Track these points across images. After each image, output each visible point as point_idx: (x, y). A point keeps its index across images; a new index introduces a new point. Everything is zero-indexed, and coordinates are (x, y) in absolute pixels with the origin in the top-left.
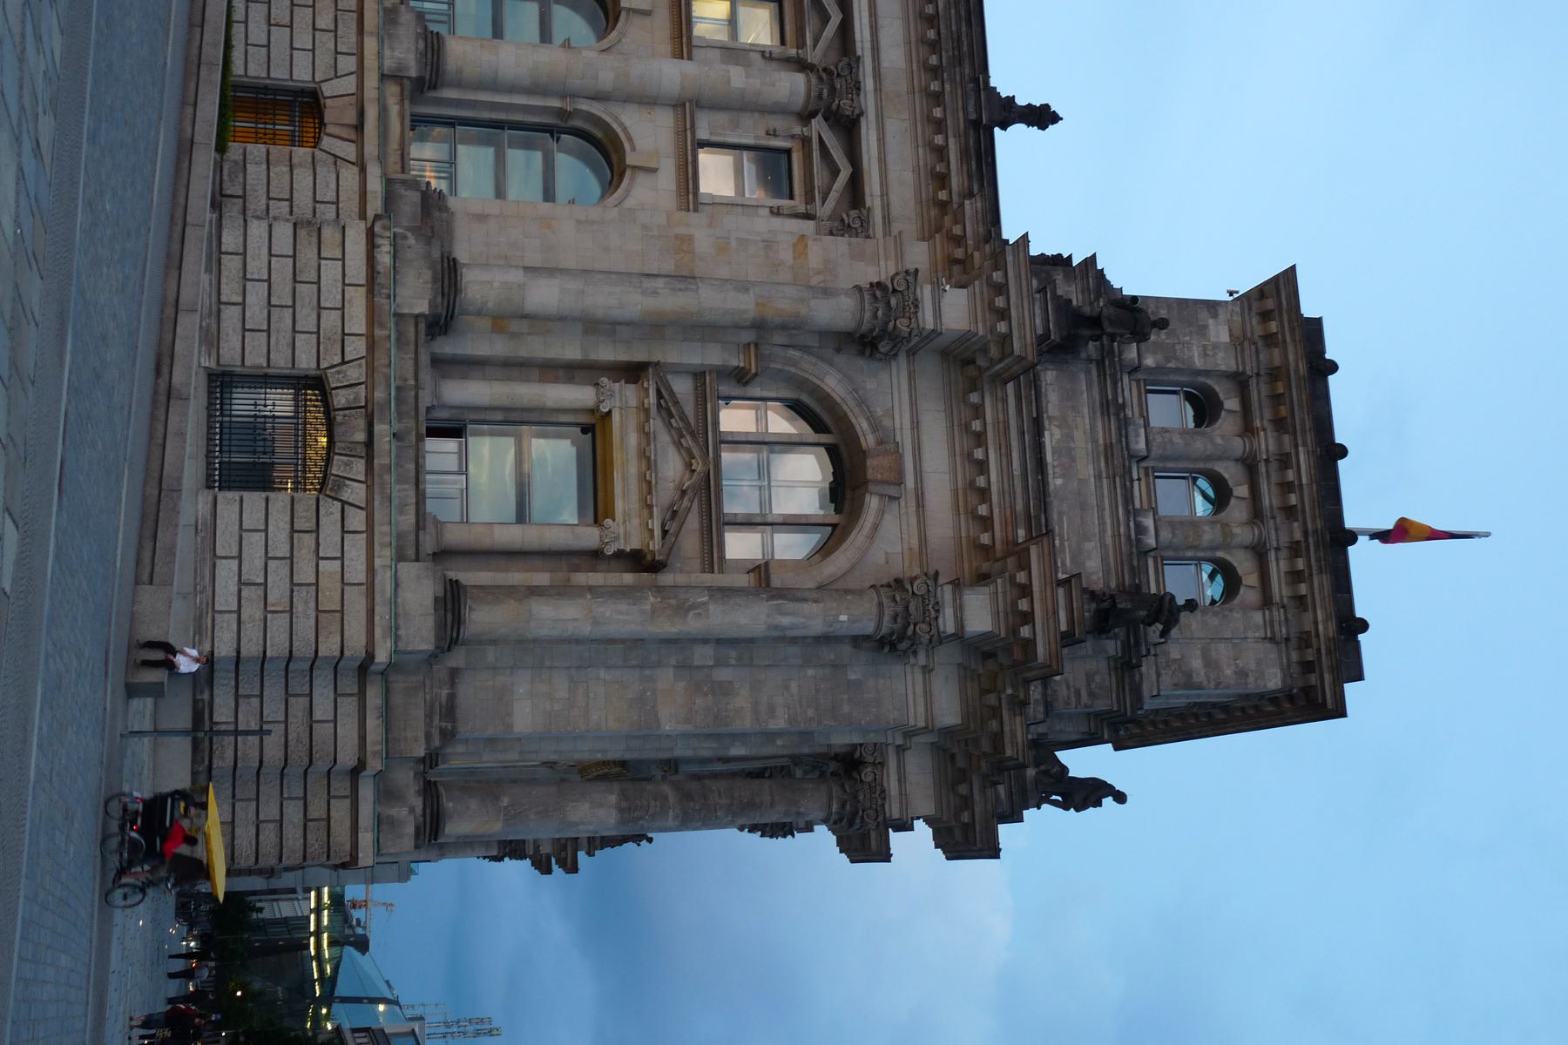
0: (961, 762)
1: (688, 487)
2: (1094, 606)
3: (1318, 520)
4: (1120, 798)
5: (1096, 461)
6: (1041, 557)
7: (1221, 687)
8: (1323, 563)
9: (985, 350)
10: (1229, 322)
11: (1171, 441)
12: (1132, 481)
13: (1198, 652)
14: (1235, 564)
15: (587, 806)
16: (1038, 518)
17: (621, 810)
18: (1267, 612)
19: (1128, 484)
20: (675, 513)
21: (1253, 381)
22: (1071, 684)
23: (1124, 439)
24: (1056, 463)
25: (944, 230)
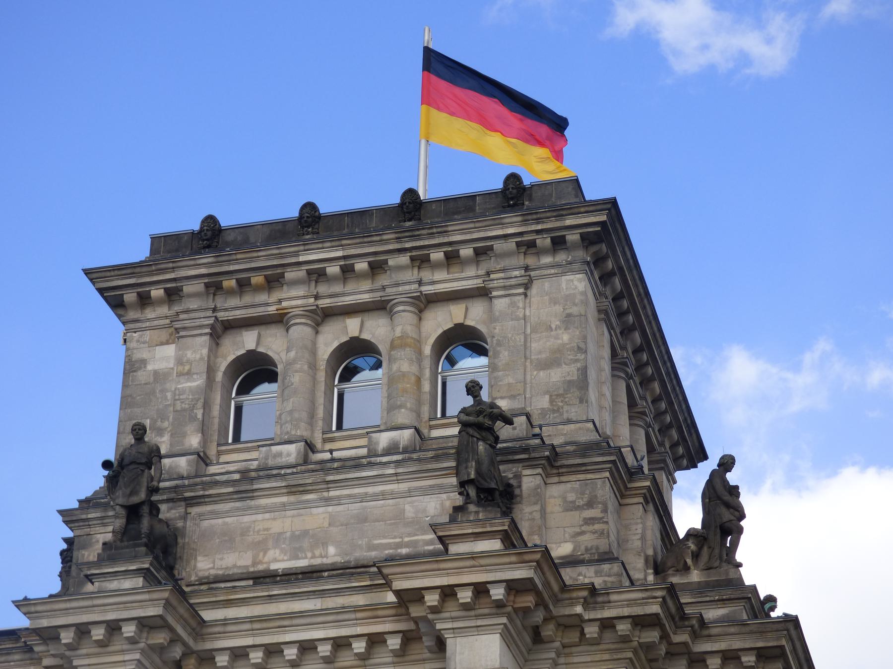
2: (472, 508)
3: (385, 237)
5: (307, 505)
6: (406, 576)
7: (582, 345)
8: (435, 230)
10: (152, 345)
12: (333, 460)
13: (542, 374)
14: (440, 331)
18: (494, 293)
19: (336, 465)
21: (222, 315)
22: (578, 530)
24: (309, 555)
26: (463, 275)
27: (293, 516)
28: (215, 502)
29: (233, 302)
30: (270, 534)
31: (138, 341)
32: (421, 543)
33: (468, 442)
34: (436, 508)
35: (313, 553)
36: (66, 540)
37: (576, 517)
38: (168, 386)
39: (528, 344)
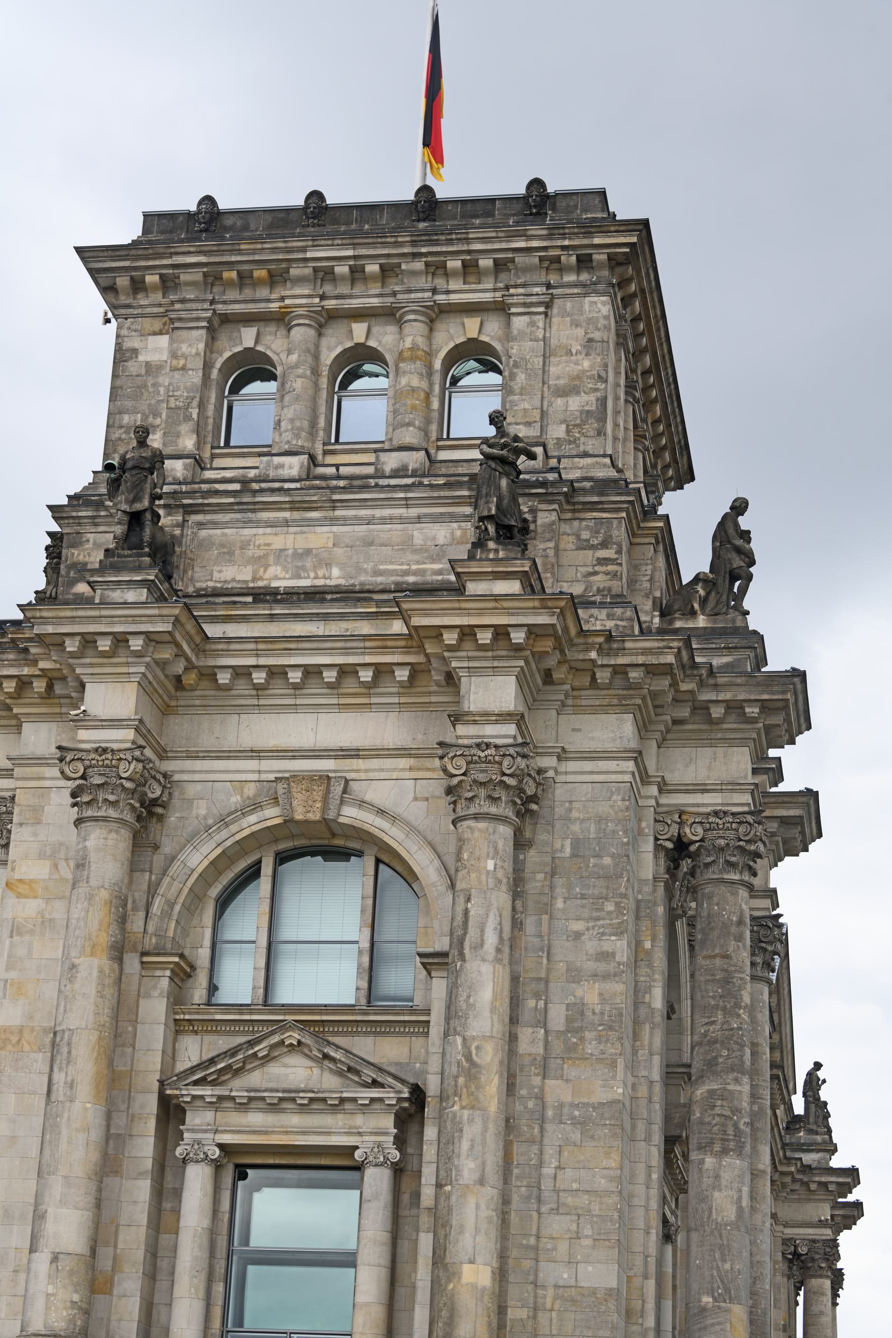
0: (684, 712)
1: (319, 1050)
2: (491, 545)
4: (739, 507)
5: (311, 523)
7: (603, 374)
8: (454, 236)
9: (162, 664)
10: (143, 335)
11: (292, 421)
14: (451, 345)
15: (717, 1194)
16: (379, 603)
17: (725, 1152)
18: (513, 310)
20: (350, 1069)
22: (590, 570)
23: (287, 485)
24: (312, 575)
25: (8, 701)
26: (480, 287)
27: (295, 533)
28: (214, 512)
29: (232, 294)
30: (271, 550)
34: (445, 537)
35: (316, 573)
36: (50, 534)
37: (589, 556)
38: (160, 379)
39: (547, 368)
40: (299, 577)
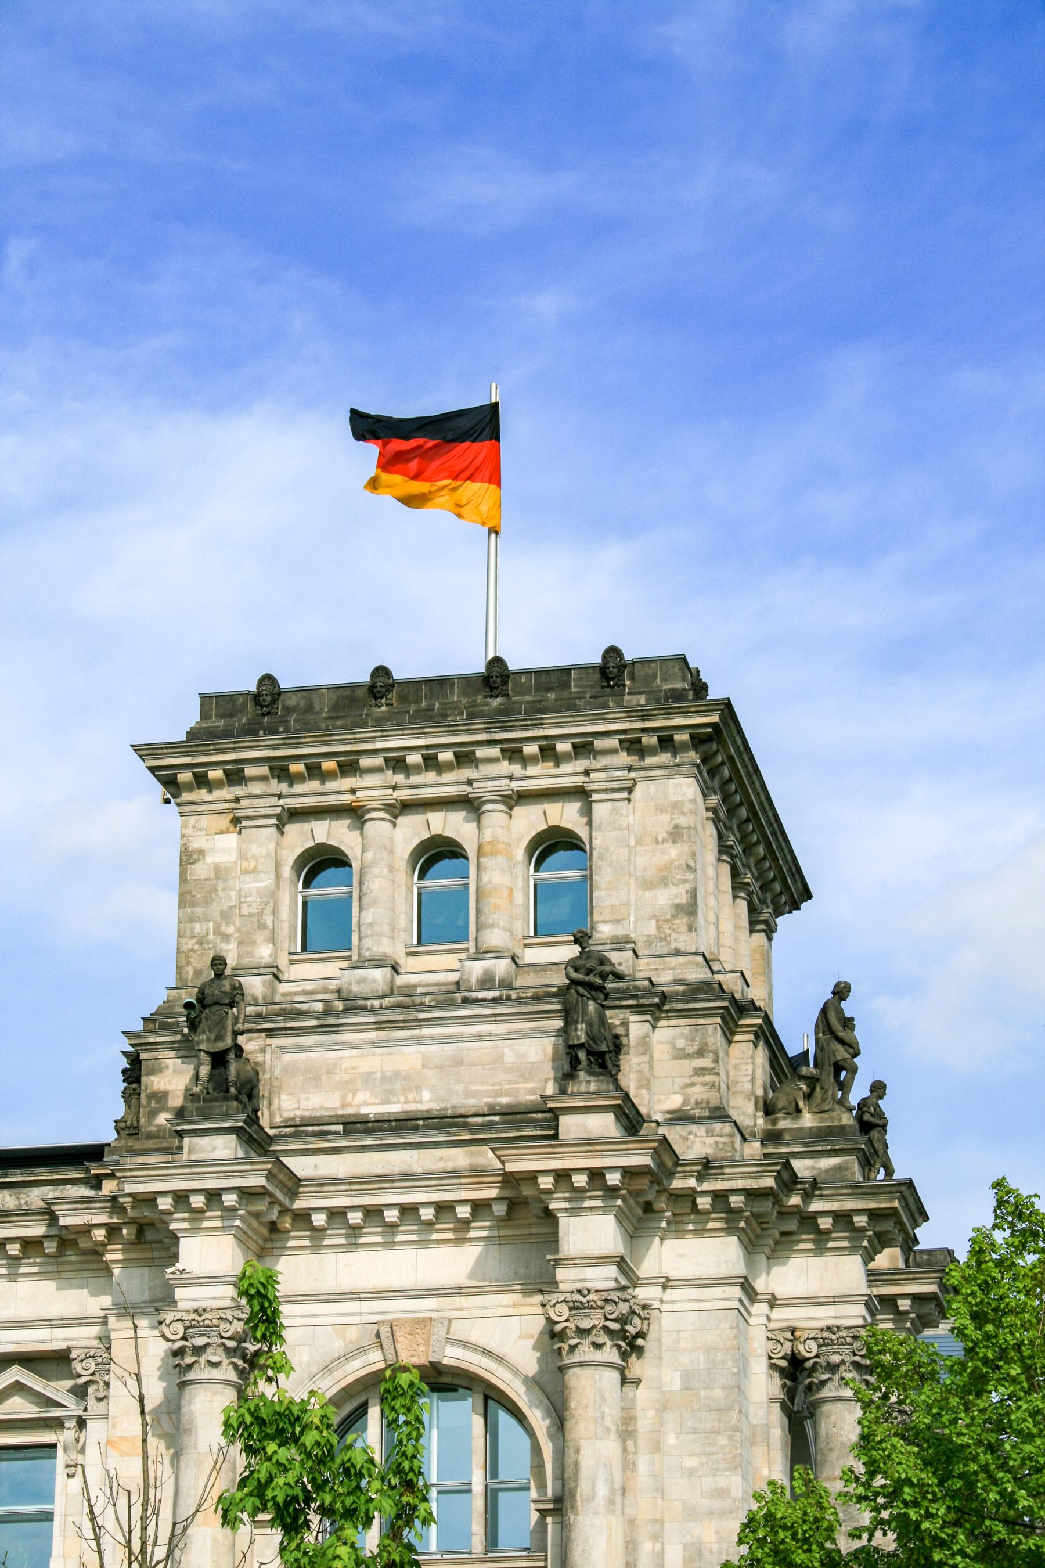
4: (841, 992)
5: (399, 1043)
7: (691, 863)
8: (529, 722)
9: (257, 1215)
14: (533, 833)
22: (687, 1081)
24: (402, 1099)
27: (382, 1055)
28: (298, 1035)
31: (194, 827)
32: (522, 1092)
33: (577, 1001)
35: (406, 1098)
36: (125, 1054)
37: (688, 1066)
38: (230, 883)
39: (633, 859)
40: (389, 1102)
